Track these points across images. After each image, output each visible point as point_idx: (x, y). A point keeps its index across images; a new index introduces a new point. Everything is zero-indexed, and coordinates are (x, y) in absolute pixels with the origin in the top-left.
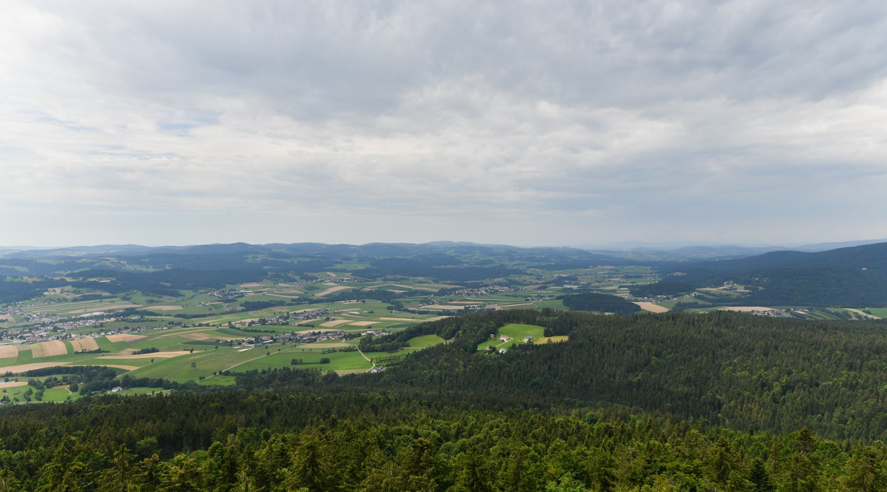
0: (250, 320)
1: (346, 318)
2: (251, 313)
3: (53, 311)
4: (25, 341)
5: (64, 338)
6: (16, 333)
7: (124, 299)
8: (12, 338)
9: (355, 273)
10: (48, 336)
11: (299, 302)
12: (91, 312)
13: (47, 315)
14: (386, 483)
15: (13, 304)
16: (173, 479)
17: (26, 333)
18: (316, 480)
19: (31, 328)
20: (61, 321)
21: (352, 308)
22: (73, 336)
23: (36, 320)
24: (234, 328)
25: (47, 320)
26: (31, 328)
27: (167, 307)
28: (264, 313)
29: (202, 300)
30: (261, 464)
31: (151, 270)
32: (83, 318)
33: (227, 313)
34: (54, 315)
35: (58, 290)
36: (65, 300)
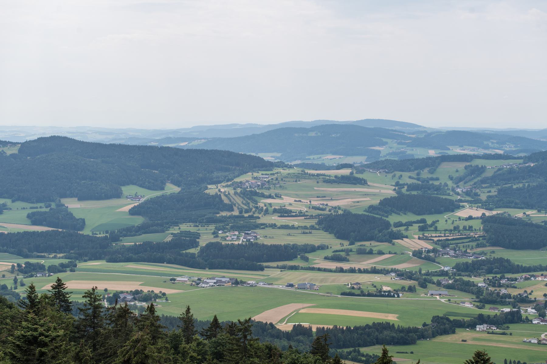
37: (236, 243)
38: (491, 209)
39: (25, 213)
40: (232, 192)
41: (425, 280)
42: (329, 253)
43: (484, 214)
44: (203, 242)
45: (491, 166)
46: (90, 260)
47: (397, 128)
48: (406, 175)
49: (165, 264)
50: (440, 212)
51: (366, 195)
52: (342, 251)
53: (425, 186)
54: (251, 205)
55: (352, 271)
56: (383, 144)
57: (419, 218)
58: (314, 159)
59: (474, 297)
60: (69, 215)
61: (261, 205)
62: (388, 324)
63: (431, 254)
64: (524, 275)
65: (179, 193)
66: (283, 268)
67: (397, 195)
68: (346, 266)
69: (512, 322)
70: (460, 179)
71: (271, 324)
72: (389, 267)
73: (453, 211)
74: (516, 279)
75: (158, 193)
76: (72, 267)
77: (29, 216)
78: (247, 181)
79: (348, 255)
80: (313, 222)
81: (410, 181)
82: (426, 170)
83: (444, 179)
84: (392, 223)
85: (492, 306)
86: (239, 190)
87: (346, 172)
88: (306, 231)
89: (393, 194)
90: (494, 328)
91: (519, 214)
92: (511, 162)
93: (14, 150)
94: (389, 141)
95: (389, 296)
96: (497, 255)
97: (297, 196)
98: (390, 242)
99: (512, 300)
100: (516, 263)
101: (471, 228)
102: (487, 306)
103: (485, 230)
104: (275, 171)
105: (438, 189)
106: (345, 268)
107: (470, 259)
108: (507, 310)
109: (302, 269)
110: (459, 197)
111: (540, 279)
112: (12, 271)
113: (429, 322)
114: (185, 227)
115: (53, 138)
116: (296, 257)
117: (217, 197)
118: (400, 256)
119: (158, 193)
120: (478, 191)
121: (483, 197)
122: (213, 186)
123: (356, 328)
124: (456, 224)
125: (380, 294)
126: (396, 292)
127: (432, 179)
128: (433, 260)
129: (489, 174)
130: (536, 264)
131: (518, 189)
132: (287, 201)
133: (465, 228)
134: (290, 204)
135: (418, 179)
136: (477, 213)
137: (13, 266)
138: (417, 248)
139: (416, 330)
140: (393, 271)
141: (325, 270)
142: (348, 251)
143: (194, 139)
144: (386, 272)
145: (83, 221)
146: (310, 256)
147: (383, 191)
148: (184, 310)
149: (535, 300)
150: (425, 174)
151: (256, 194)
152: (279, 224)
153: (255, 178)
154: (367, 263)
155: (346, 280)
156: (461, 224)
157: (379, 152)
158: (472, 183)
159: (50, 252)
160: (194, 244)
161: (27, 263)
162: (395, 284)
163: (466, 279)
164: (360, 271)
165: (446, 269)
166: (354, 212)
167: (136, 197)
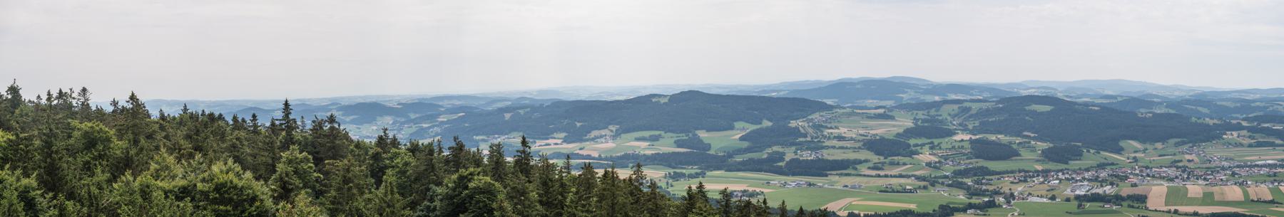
4: (1208, 183)
5: (1241, 184)
6: (1200, 174)
8: (1197, 179)
10: (1227, 181)
12: (1265, 160)
13: (1226, 159)
15: (1197, 144)
17: (1209, 175)
19: (1214, 171)
20: (1238, 166)
22: (1249, 183)
23: (1217, 162)
25: (1226, 164)
26: (1214, 171)
32: (1257, 166)
34: (1232, 159)
35: (1235, 134)
36: (1242, 145)
37: (809, 158)
38: (975, 135)
40: (806, 125)
41: (934, 181)
42: (871, 165)
43: (971, 138)
44: (787, 158)
45: (975, 107)
46: (714, 170)
47: (914, 82)
48: (920, 113)
49: (763, 173)
51: (894, 126)
53: (932, 120)
54: (819, 133)
55: (886, 176)
56: (904, 92)
57: (929, 141)
58: (860, 103)
59: (965, 191)
60: (700, 141)
61: (825, 133)
62: (910, 210)
63: (938, 165)
64: (997, 177)
65: (772, 126)
66: (841, 175)
68: (882, 173)
69: (990, 207)
70: (955, 115)
71: (833, 212)
72: (910, 173)
73: (951, 136)
74: (992, 180)
75: (759, 126)
76: (703, 175)
77: (675, 142)
78: (816, 118)
79: (883, 165)
80: (860, 144)
81: (923, 117)
82: (934, 109)
83: (945, 116)
84: (912, 144)
85: (976, 197)
86: (811, 124)
87: (881, 111)
88: (855, 149)
89: (912, 125)
91: (993, 138)
92: (988, 104)
93: (666, 100)
94: (909, 90)
95: (910, 192)
96: (979, 165)
97: (850, 127)
98: (910, 157)
99: (989, 193)
100: (992, 169)
101: (962, 147)
103: (972, 148)
104: (834, 111)
105: (941, 122)
106: (881, 175)
107: (963, 167)
108: (986, 199)
109: (853, 175)
110: (955, 127)
112: (665, 177)
113: (937, 209)
114: (776, 148)
115: (690, 91)
116: (849, 167)
117: (797, 128)
119: (759, 126)
120: (967, 123)
121: (970, 127)
122: (794, 122)
124: (953, 144)
125: (905, 191)
126: (915, 189)
127: (937, 115)
128: (938, 168)
129: (973, 112)
130: (1004, 170)
131: (992, 122)
132: (843, 131)
134: (845, 133)
135: (928, 115)
136: (967, 137)
137: (666, 174)
138: (928, 160)
141: (868, 176)
142: (883, 163)
143: (781, 91)
144: (908, 177)
145: (710, 145)
146: (858, 167)
147: (906, 124)
148: (781, 203)
149: (1004, 193)
150: (933, 112)
151: (822, 126)
152: (837, 146)
153: (822, 116)
154: (896, 171)
156: (957, 145)
157: (902, 98)
158: (963, 118)
159: (689, 165)
160: (782, 160)
161: (674, 172)
162: (914, 185)
163: (960, 180)
164: (891, 176)
165: (947, 174)
166: (887, 137)
167: (743, 129)
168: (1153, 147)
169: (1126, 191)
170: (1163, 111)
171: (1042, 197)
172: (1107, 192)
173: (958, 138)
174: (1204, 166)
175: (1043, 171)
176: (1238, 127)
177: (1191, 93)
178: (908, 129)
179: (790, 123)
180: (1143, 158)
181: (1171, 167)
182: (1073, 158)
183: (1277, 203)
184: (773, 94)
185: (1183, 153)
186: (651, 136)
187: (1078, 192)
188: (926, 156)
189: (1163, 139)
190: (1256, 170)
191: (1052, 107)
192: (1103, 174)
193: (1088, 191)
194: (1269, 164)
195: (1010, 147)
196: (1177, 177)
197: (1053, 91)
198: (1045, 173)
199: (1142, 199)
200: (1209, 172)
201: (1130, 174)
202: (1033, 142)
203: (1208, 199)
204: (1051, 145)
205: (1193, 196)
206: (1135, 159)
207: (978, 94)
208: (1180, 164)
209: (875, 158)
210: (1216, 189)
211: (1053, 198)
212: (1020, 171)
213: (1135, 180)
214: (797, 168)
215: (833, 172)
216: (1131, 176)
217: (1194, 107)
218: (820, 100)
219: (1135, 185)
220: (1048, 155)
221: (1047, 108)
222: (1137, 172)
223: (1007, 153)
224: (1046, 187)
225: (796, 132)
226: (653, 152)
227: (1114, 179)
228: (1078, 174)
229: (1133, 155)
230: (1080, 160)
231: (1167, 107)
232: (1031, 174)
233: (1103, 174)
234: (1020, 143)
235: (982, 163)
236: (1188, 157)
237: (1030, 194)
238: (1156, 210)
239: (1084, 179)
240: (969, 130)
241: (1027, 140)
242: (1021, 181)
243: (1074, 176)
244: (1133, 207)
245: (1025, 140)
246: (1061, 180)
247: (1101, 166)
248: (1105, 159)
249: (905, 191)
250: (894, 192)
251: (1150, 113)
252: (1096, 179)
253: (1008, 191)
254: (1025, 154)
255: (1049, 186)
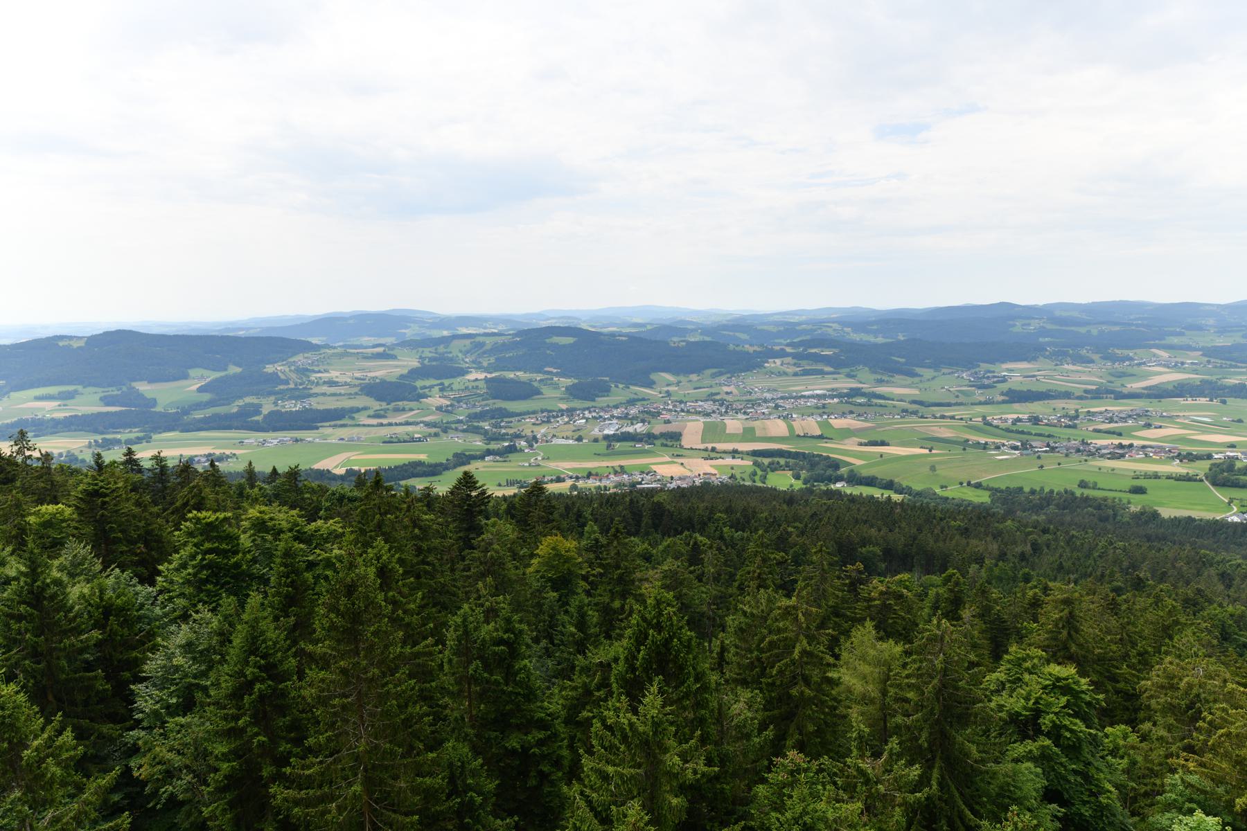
0: (1015, 416)
1: (1185, 427)
2: (1016, 406)
3: (774, 385)
5: (785, 418)
7: (849, 376)
9: (1210, 352)
10: (770, 414)
11: (1097, 394)
12: (813, 390)
13: (769, 390)
14: (1188, 683)
16: (873, 594)
17: (749, 408)
18: (1074, 648)
19: (755, 403)
20: (782, 398)
21: (1200, 410)
22: (794, 416)
24: (991, 425)
25: (768, 396)
26: (755, 403)
27: (900, 389)
28: (1037, 408)
29: (946, 384)
30: (998, 608)
31: (880, 340)
32: (804, 397)
33: (980, 403)
34: (775, 390)
35: (778, 361)
36: (785, 374)
37: (294, 409)
38: (491, 373)
39: (97, 397)
40: (287, 369)
41: (446, 427)
42: (371, 412)
45: (489, 341)
46: (164, 431)
47: (418, 315)
48: (427, 350)
50: (453, 377)
51: (397, 367)
52: (381, 410)
54: (304, 379)
55: (390, 424)
56: (407, 328)
57: (439, 382)
60: (140, 396)
64: (517, 418)
66: (335, 426)
67: (420, 366)
68: (385, 421)
70: (467, 352)
71: (328, 470)
72: (419, 420)
73: (463, 375)
74: (511, 422)
75: (222, 374)
77: (101, 399)
80: (356, 390)
81: (430, 355)
82: (442, 346)
86: (293, 368)
87: (380, 350)
90: (498, 458)
91: (511, 375)
92: (503, 338)
93: (81, 343)
94: (412, 325)
97: (342, 370)
98: (418, 401)
101: (477, 386)
102: (492, 442)
103: (487, 388)
105: (451, 359)
107: (478, 410)
108: (506, 444)
109: (351, 426)
111: (528, 420)
112: (90, 446)
113: (451, 458)
114: (248, 400)
117: (275, 374)
118: (426, 410)
119: (222, 374)
121: (485, 364)
122: (271, 366)
123: (396, 467)
124: (466, 385)
125: (413, 440)
126: (425, 437)
127: (447, 353)
129: (488, 347)
130: (525, 410)
131: (509, 357)
132: (334, 374)
133: (473, 387)
134: (337, 377)
135: (436, 353)
136: (481, 376)
137: (90, 443)
139: (441, 464)
140: (421, 422)
142: (386, 410)
144: (416, 424)
145: (155, 400)
146: (356, 415)
150: (441, 349)
151: (307, 370)
152: (328, 393)
155: (386, 432)
156: (470, 385)
157: (405, 333)
160: (258, 412)
163: (476, 424)
165: (461, 418)
166: (388, 380)
168: (688, 379)
169: (658, 428)
170: (697, 339)
171: (567, 438)
172: (638, 430)
173: (472, 376)
174: (744, 398)
175: (568, 410)
176: (782, 354)
177: (729, 318)
178: (412, 369)
179: (265, 368)
180: (676, 392)
181: (707, 400)
182: (600, 394)
183: (826, 438)
184: (241, 333)
185: (720, 385)
186: (60, 393)
187: (606, 432)
188: (436, 400)
189: (698, 370)
190: (802, 401)
191: (575, 339)
192: (633, 411)
193: (617, 430)
194: (817, 395)
195: (530, 384)
196: (714, 412)
197: (576, 321)
198: (570, 412)
199: (676, 437)
200: (749, 405)
201: (662, 409)
202: (555, 379)
203: (748, 434)
204: (576, 381)
205: (732, 432)
206: (668, 394)
207: (492, 326)
208: (718, 397)
209: (376, 405)
210: (757, 424)
211: (580, 439)
212: (542, 411)
213: (668, 417)
214: (278, 422)
215: (328, 424)
216: (664, 412)
217: (731, 333)
218: (303, 339)
219: (668, 422)
220: (574, 392)
221: (570, 340)
222: (670, 407)
223: (527, 392)
224: (571, 427)
225: (274, 378)
226: (67, 415)
227: (646, 415)
228: (606, 411)
229: (666, 389)
230: (608, 396)
231: (701, 334)
232: (555, 413)
233: (633, 411)
234: (541, 381)
235: (500, 404)
236: (726, 389)
237: (554, 436)
238: (692, 449)
239: (613, 417)
240: (484, 368)
241: (549, 377)
242: (543, 422)
243: (602, 414)
244: (666, 446)
245: (546, 376)
246: (587, 419)
247: (632, 402)
248: (636, 394)
249: (413, 440)
250: (401, 442)
251: (682, 341)
252: (625, 417)
253: (529, 434)
254: (548, 392)
255: (575, 426)
